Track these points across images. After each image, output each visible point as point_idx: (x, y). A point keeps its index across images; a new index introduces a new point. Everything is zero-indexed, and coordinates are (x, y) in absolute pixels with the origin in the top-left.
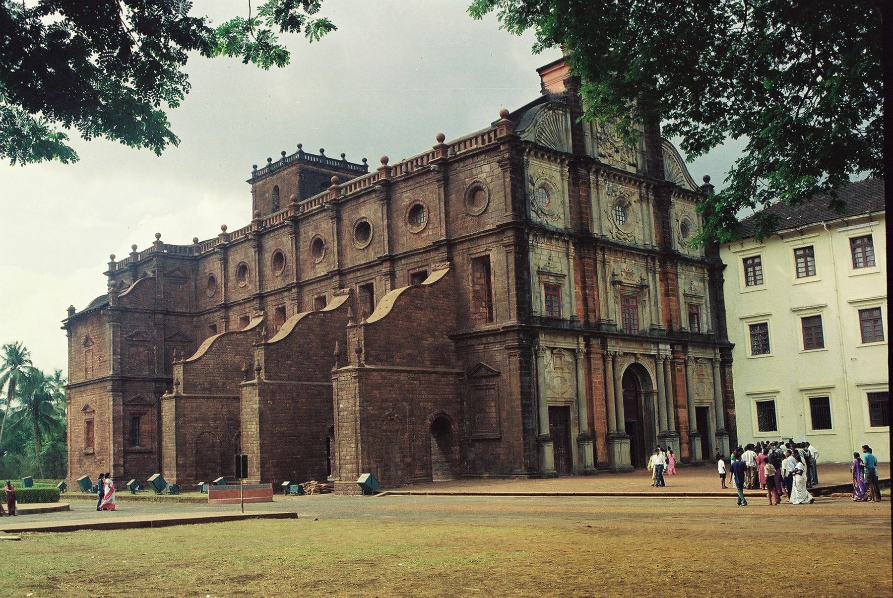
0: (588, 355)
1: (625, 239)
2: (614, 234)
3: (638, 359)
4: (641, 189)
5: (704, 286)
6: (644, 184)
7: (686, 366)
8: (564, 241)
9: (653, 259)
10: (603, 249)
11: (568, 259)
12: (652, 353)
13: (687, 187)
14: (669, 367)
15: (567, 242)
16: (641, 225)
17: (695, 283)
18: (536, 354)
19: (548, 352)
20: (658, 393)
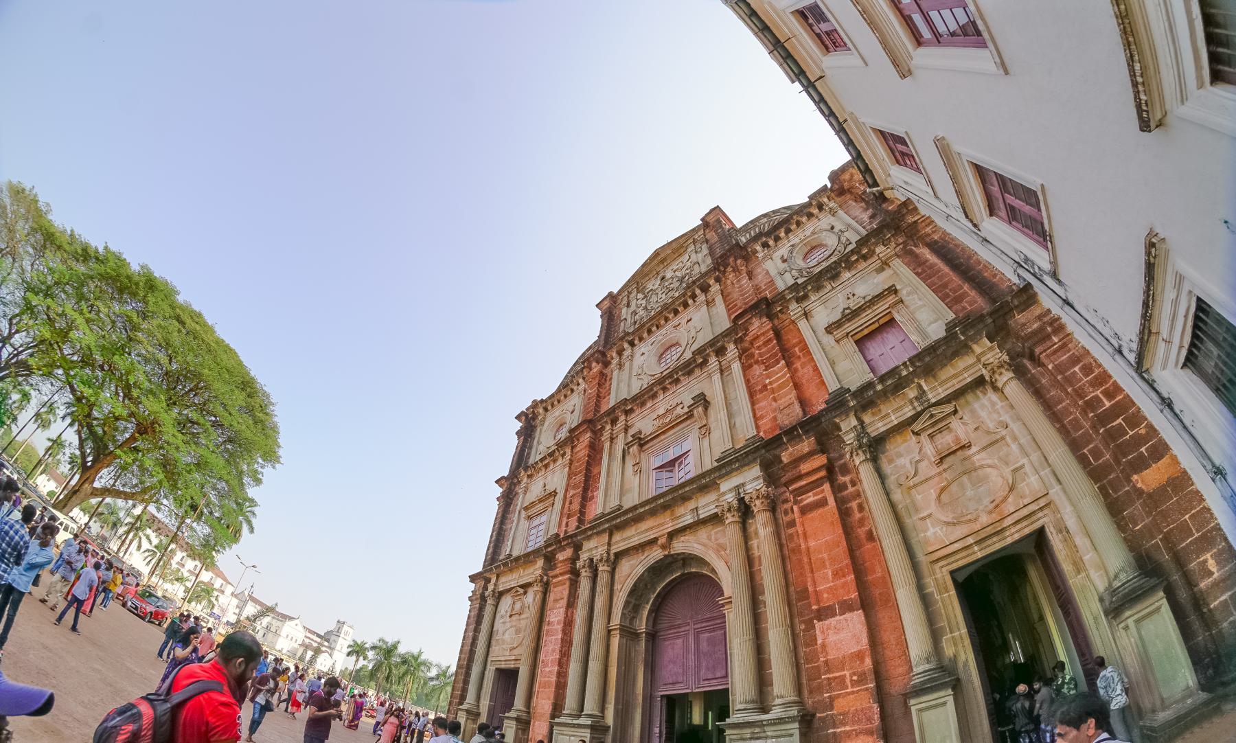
10: (614, 422)
12: (701, 517)
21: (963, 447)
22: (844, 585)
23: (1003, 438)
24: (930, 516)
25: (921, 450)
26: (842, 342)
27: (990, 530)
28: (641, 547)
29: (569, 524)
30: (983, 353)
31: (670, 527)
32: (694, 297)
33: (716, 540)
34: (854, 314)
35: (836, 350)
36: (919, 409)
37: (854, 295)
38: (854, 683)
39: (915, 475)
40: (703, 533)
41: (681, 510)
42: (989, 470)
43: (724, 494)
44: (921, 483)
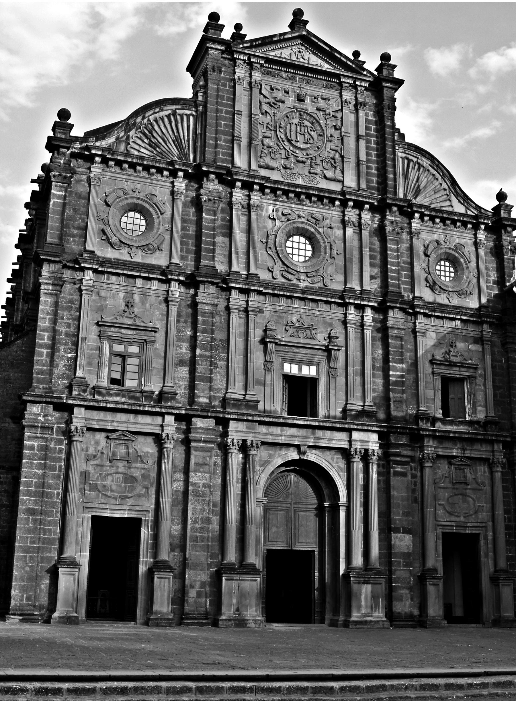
1: (299, 280)
2: (277, 273)
3: (304, 453)
4: (343, 212)
5: (483, 348)
6: (351, 204)
7: (422, 468)
9: (360, 308)
11: (168, 307)
13: (459, 208)
14: (374, 469)
15: (168, 282)
16: (340, 260)
17: (461, 345)
22: (406, 520)
23: (481, 490)
25: (449, 472)
27: (462, 524)
29: (198, 387)
30: (497, 451)
32: (344, 204)
33: (337, 463)
35: (430, 378)
36: (459, 455)
37: (455, 346)
38: (404, 566)
40: (328, 454)
41: (320, 433)
42: (471, 499)
43: (356, 441)
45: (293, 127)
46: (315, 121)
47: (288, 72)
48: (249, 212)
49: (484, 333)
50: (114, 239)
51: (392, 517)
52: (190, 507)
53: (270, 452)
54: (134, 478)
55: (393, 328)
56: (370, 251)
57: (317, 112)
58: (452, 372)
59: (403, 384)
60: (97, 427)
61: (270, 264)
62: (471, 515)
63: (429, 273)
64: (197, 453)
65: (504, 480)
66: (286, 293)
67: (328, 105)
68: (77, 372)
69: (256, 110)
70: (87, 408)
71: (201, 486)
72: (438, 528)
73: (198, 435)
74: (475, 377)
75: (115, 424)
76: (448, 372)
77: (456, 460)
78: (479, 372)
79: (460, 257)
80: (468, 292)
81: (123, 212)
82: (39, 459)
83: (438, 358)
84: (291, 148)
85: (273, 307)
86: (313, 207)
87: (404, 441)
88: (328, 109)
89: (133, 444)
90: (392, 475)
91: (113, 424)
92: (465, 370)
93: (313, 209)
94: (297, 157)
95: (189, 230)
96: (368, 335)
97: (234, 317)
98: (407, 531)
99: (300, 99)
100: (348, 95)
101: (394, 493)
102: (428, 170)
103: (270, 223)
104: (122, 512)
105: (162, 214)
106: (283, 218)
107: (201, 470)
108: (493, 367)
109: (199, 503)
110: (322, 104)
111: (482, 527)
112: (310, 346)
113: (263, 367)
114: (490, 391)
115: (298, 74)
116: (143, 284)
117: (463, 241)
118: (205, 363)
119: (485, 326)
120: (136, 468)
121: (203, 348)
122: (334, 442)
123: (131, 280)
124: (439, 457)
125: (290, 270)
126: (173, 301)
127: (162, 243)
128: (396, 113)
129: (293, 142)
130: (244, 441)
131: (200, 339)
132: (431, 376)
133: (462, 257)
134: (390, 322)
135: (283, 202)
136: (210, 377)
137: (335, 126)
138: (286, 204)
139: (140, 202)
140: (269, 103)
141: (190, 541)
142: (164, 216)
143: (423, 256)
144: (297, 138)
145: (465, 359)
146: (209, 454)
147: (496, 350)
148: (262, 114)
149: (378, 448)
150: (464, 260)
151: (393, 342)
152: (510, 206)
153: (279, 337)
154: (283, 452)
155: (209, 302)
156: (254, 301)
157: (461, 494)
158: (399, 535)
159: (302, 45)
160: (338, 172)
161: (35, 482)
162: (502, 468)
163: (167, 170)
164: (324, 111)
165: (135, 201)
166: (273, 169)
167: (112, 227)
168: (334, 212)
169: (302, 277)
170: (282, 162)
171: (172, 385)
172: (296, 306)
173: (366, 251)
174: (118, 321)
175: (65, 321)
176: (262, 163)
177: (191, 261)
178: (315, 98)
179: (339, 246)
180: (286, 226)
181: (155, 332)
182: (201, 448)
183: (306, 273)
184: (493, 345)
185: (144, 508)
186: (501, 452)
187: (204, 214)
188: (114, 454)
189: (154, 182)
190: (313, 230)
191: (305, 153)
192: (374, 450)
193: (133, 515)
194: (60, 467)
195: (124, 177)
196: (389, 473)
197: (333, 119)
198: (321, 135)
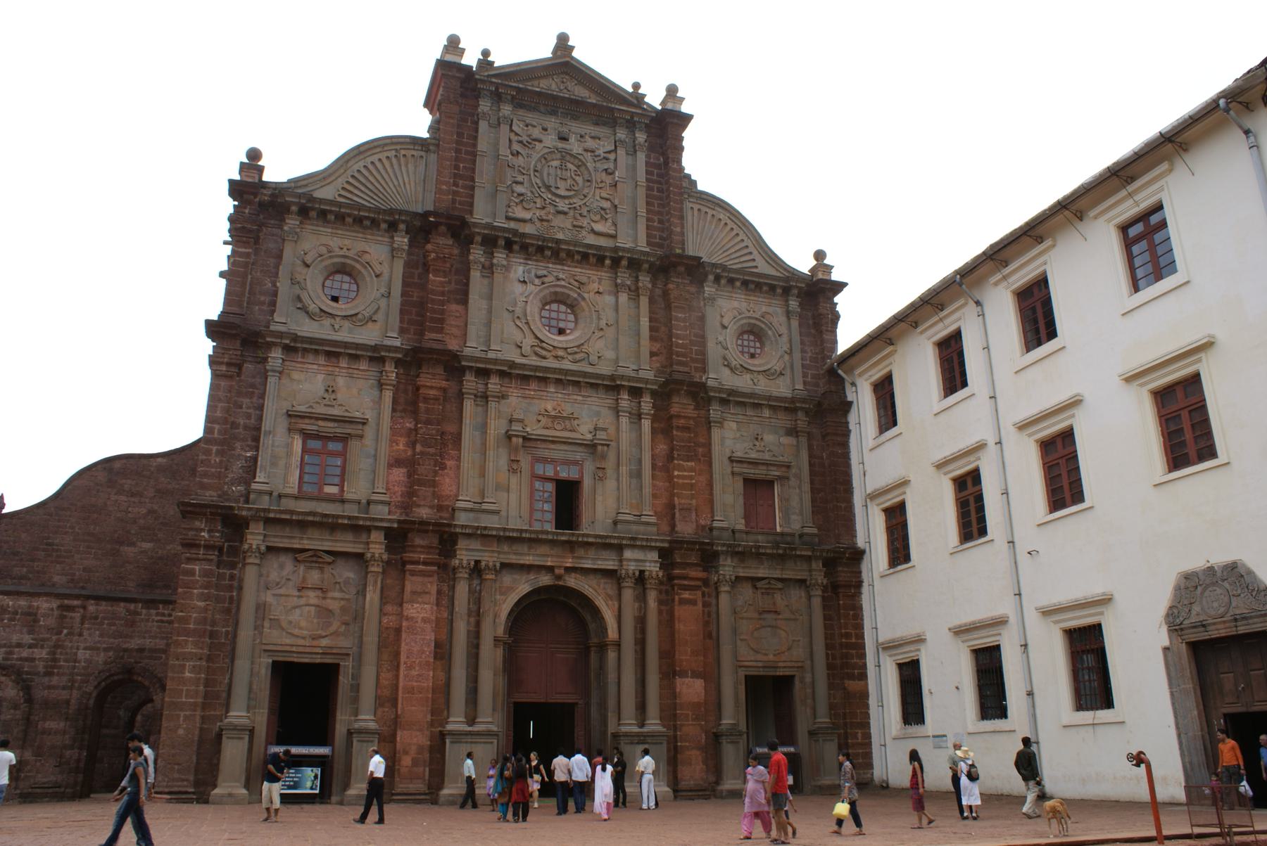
0: (398, 565)
1: (556, 357)
2: (527, 349)
4: (616, 274)
5: (798, 442)
6: (624, 263)
7: (718, 594)
8: (371, 359)
9: (636, 393)
10: (483, 373)
11: (381, 391)
14: (652, 597)
15: (382, 360)
16: (610, 333)
17: (769, 438)
18: (244, 558)
19: (287, 561)
20: (619, 645)
21: (776, 612)
23: (796, 620)
24: (745, 640)
26: (737, 478)
28: (528, 568)
30: (816, 570)
31: (569, 563)
32: (616, 262)
33: (604, 589)
34: (754, 463)
39: (745, 612)
41: (581, 552)
42: (782, 632)
43: (630, 560)
44: (747, 618)
45: (552, 171)
46: (581, 165)
47: (547, 105)
48: (493, 273)
49: (799, 422)
50: (312, 307)
51: (677, 657)
52: (404, 648)
53: (517, 577)
54: (330, 611)
55: (679, 417)
56: (650, 321)
57: (585, 153)
58: (757, 471)
59: (692, 485)
60: (281, 545)
61: (518, 336)
62: (783, 653)
63: (727, 349)
64: (414, 578)
65: (825, 607)
66: (538, 374)
67: (599, 145)
68: (258, 474)
69: (504, 151)
70: (268, 522)
71: (419, 621)
72: (740, 670)
73: (416, 556)
74: (788, 478)
75: (305, 542)
76: (752, 471)
77: (763, 582)
78: (794, 471)
79: (767, 329)
80: (778, 372)
81: (326, 274)
82: (201, 588)
83: (739, 454)
84: (550, 196)
85: (522, 391)
86: (576, 267)
87: (693, 560)
88: (598, 149)
89: (332, 566)
90: (676, 603)
91: (302, 542)
92: (775, 468)
93: (576, 270)
94: (556, 206)
95: (412, 296)
96: (646, 425)
97: (469, 403)
98: (696, 675)
99: (563, 139)
100: (622, 134)
101: (680, 626)
102: (726, 224)
103: (520, 285)
104: (314, 656)
105: (377, 276)
106: (537, 281)
107: (420, 600)
108: (811, 465)
109: (416, 642)
110: (590, 144)
111: (798, 667)
112: (570, 441)
113: (506, 468)
114: (807, 497)
115: (559, 108)
116: (348, 364)
117: (770, 310)
118: (427, 463)
119: (800, 415)
120: (333, 598)
121: (426, 444)
122: (600, 562)
123: (334, 360)
124: (736, 577)
125: (544, 345)
126: (387, 385)
127: (376, 312)
128: (684, 154)
129: (553, 189)
130: (477, 562)
131: (421, 431)
132: (730, 477)
133: (770, 329)
134: (675, 409)
135: (537, 261)
136: (434, 481)
137: (606, 170)
138: (541, 264)
139: (349, 261)
140: (520, 142)
141: (403, 693)
142: (381, 278)
143: (719, 329)
144: (556, 183)
145: (774, 455)
146: (431, 579)
147: (815, 443)
148: (513, 155)
149: (658, 569)
150: (774, 334)
151: (679, 434)
152: (829, 265)
153: (528, 429)
154: (532, 576)
155: (434, 385)
156: (495, 384)
157: (769, 626)
158: (687, 680)
159: (567, 74)
160: (609, 223)
161: (195, 618)
162: (823, 592)
163: (385, 221)
164: (593, 152)
165: (342, 260)
166: (524, 221)
167: (311, 293)
168: (603, 274)
169: (560, 353)
170: (538, 213)
171: (385, 491)
172: (552, 390)
173: (645, 322)
174: (313, 411)
175: (244, 410)
176: (510, 214)
177: (415, 334)
178: (581, 136)
179: (608, 316)
180: (541, 291)
181: (364, 424)
182: (419, 571)
183: (566, 349)
184: (810, 436)
185: (344, 651)
186: (820, 571)
187: (431, 275)
188: (304, 579)
189: (369, 237)
190: (575, 295)
191: (567, 201)
192: (651, 571)
193: (328, 660)
194: (231, 598)
195: (330, 230)
196: (673, 600)
197: (605, 161)
198: (588, 181)
